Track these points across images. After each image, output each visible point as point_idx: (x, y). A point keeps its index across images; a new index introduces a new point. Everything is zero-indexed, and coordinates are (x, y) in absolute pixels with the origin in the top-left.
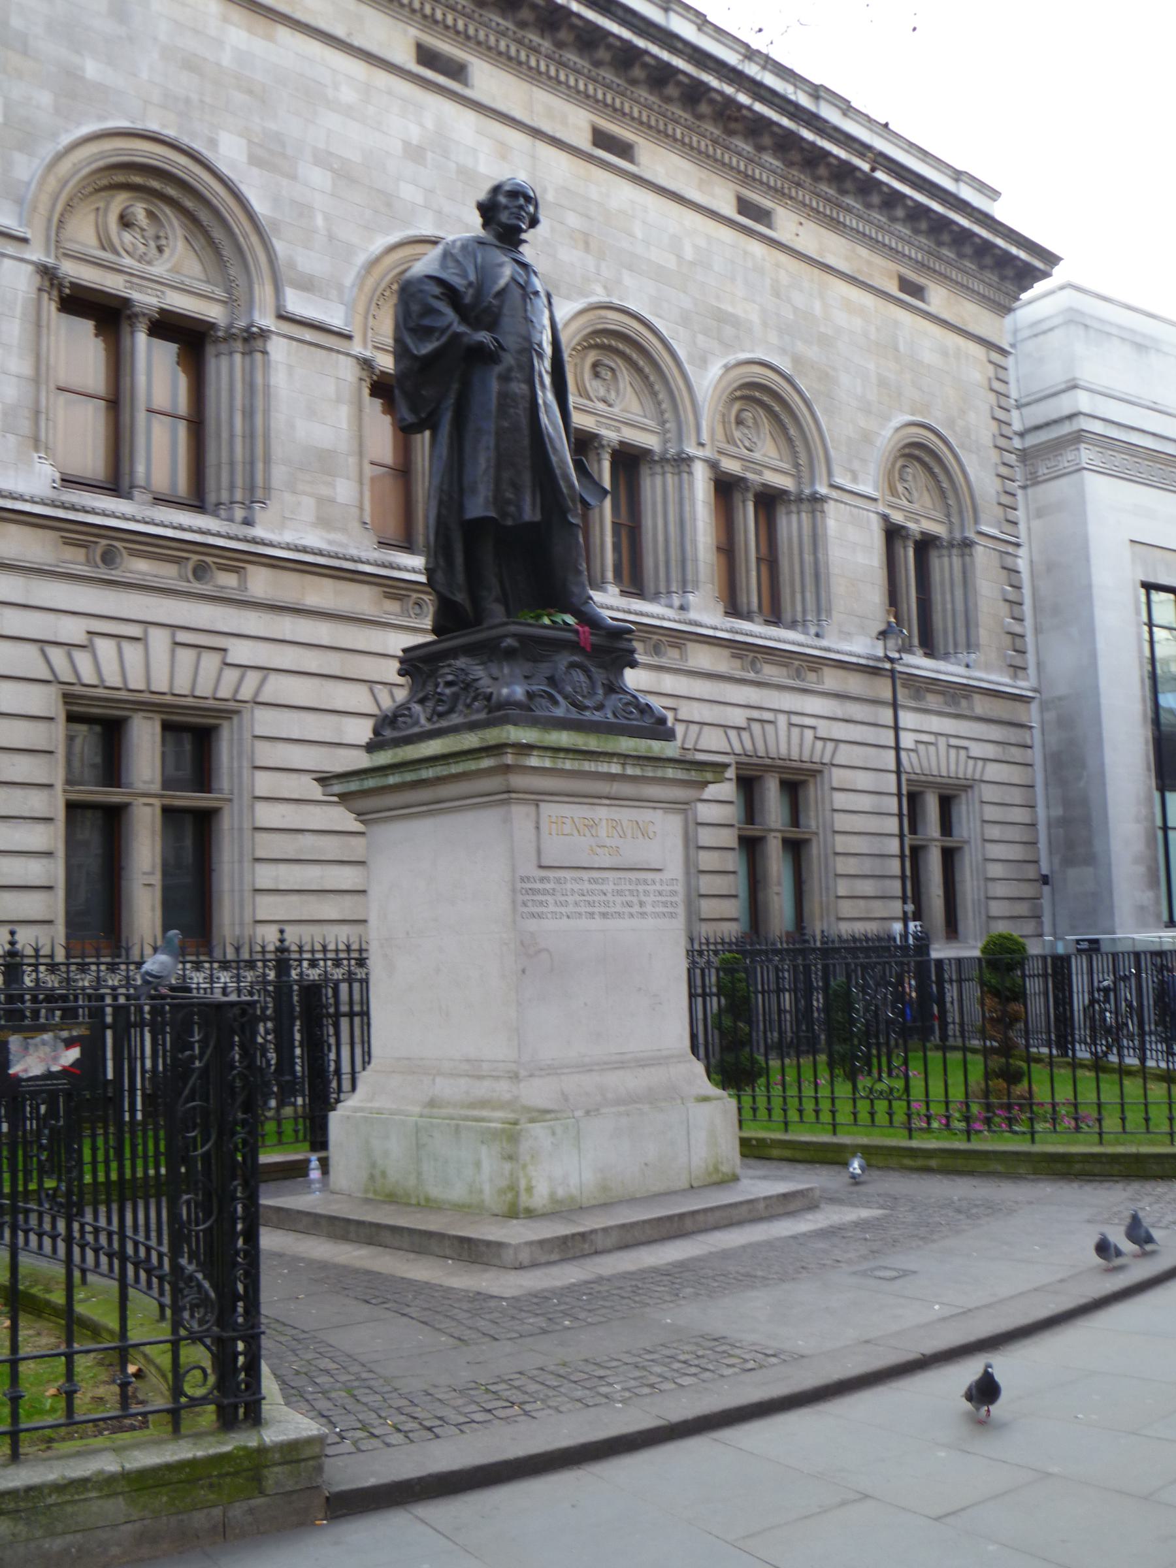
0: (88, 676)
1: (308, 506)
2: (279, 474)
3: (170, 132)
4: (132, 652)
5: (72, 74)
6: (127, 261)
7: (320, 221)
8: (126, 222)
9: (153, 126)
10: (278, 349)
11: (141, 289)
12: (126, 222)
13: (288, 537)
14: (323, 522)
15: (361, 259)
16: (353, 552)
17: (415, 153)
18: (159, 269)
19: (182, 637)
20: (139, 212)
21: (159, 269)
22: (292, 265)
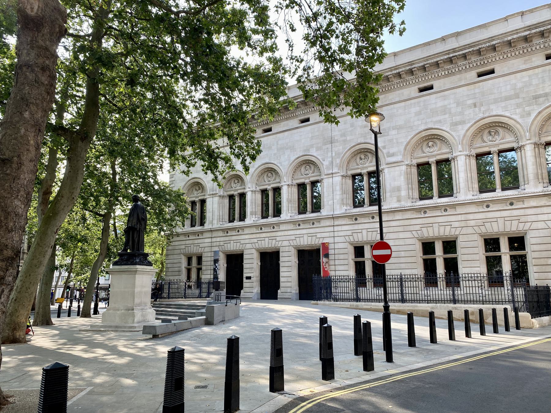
0: (352, 240)
1: (395, 199)
2: (388, 195)
3: (363, 141)
4: (360, 235)
5: (345, 141)
6: (361, 166)
7: (395, 141)
8: (361, 159)
9: (359, 141)
10: (386, 171)
11: (363, 170)
12: (361, 159)
13: (390, 207)
14: (399, 201)
15: (405, 143)
16: (406, 205)
17: (418, 113)
18: (367, 165)
19: (369, 230)
20: (363, 157)
21: (367, 165)
22: (389, 153)
